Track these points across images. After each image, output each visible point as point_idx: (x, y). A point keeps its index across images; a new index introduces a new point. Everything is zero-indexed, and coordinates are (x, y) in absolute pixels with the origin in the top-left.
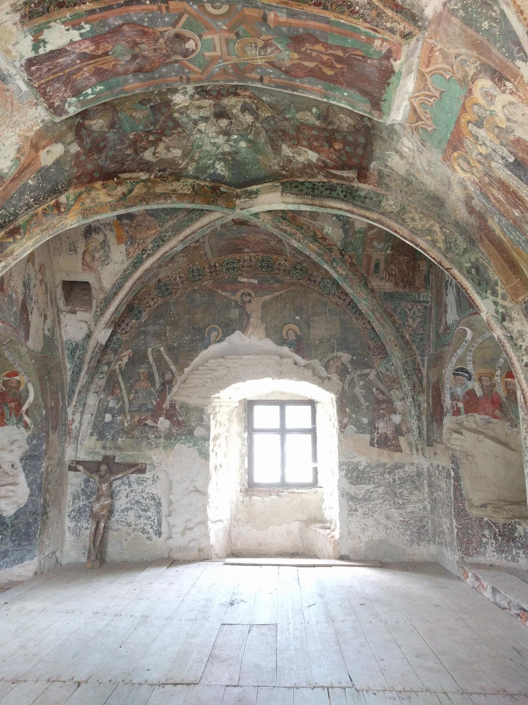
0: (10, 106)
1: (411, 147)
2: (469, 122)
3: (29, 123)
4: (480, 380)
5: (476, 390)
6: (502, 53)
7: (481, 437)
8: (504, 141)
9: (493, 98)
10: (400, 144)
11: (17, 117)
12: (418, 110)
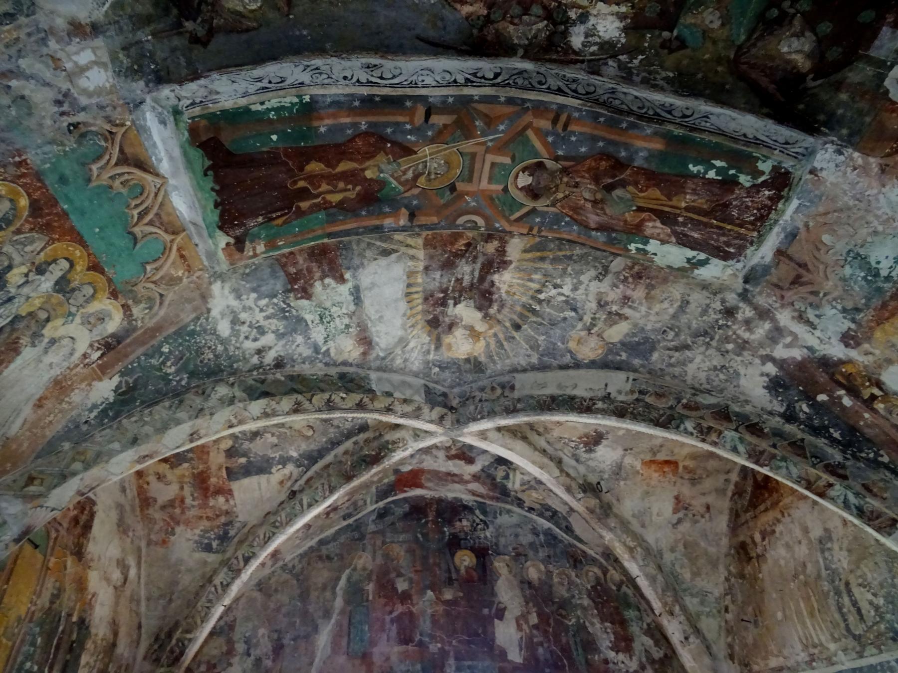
0: (830, 216)
1: (83, 82)
2: (72, 265)
3: (852, 176)
6: (133, 362)
8: (21, 325)
9: (89, 327)
10: (106, 59)
11: (846, 199)
12: (138, 173)
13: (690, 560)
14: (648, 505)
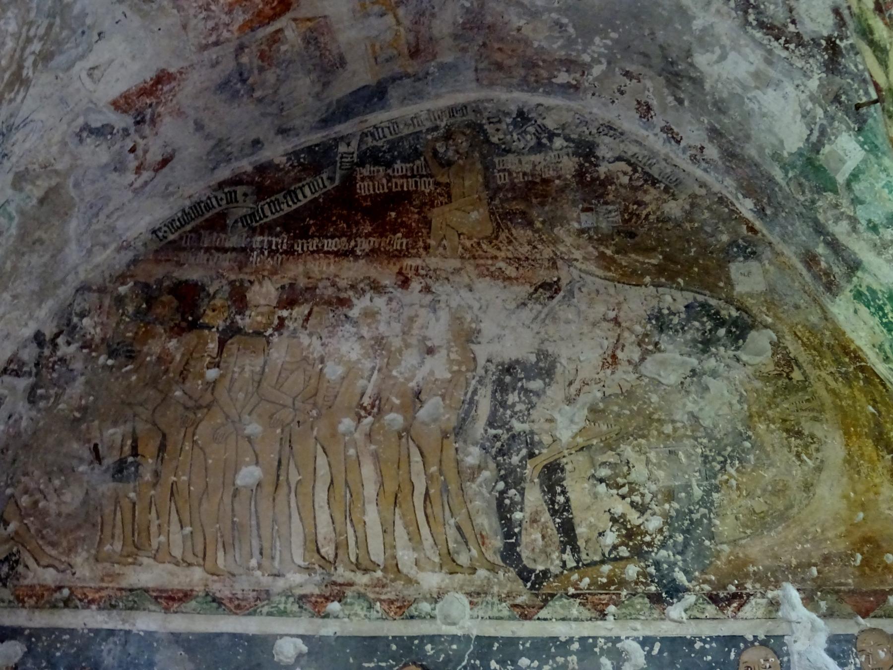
13: (22, 236)
14: (107, 25)
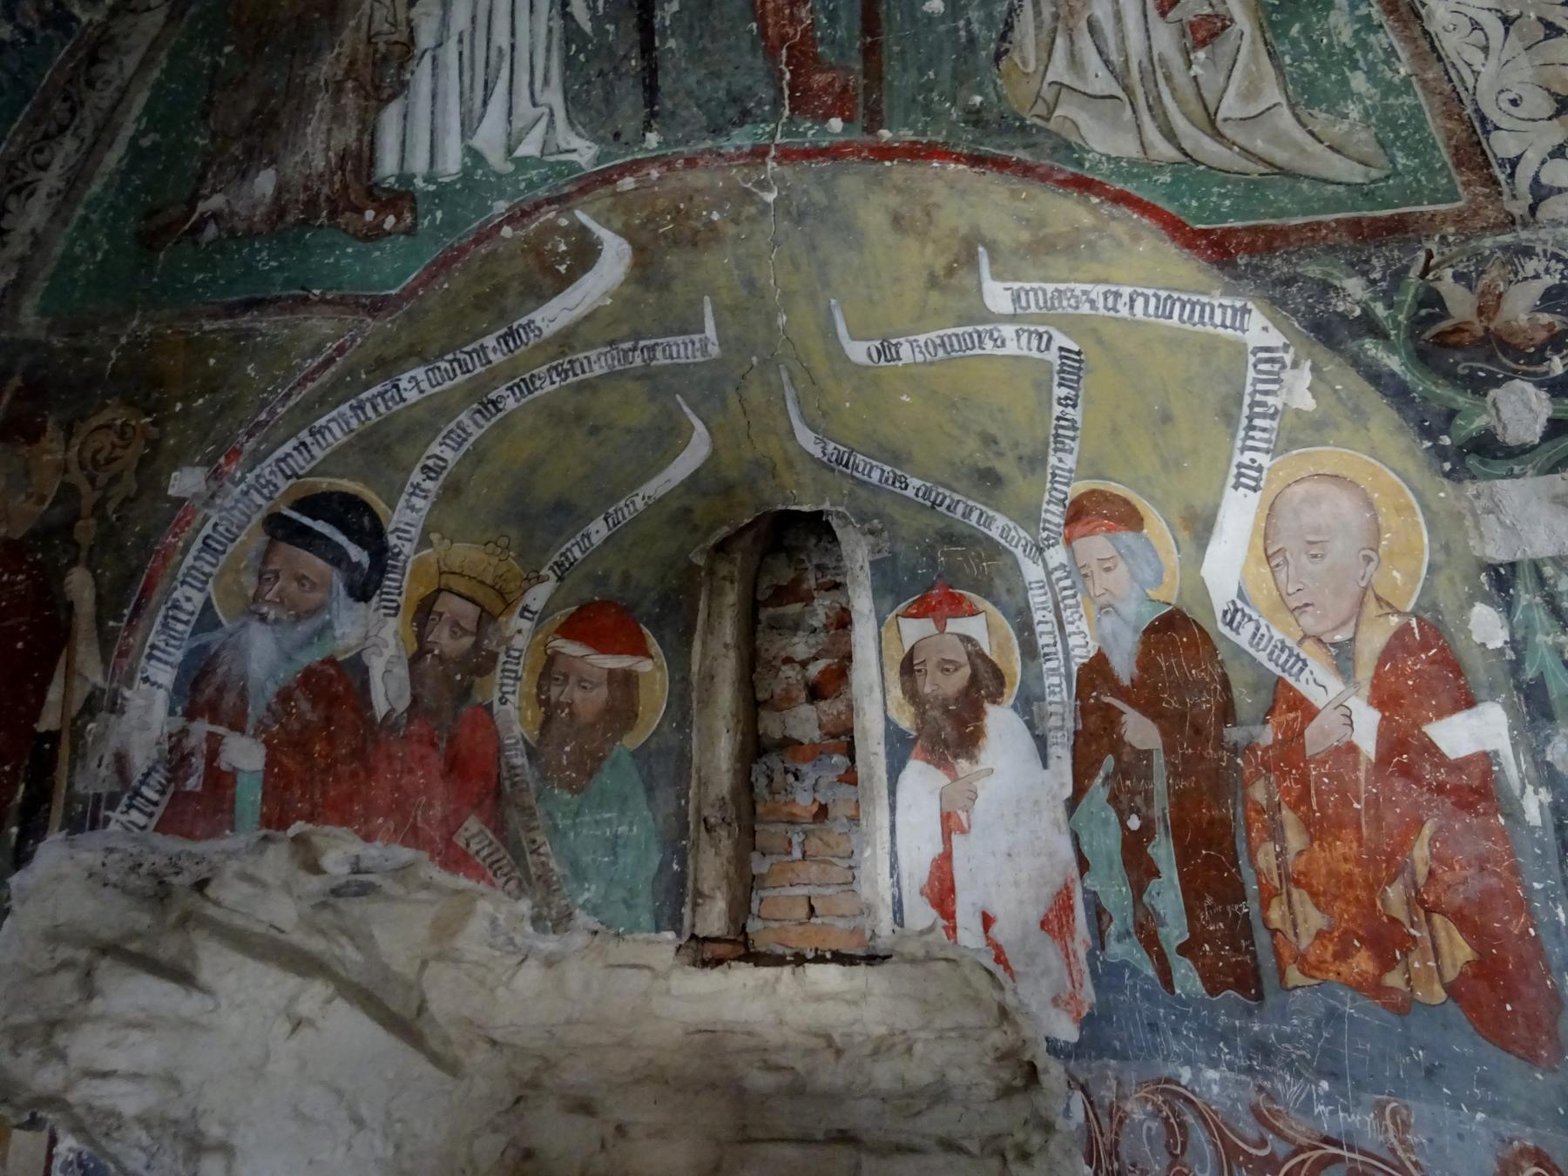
4: (425, 612)
5: (377, 666)
7: (313, 995)
